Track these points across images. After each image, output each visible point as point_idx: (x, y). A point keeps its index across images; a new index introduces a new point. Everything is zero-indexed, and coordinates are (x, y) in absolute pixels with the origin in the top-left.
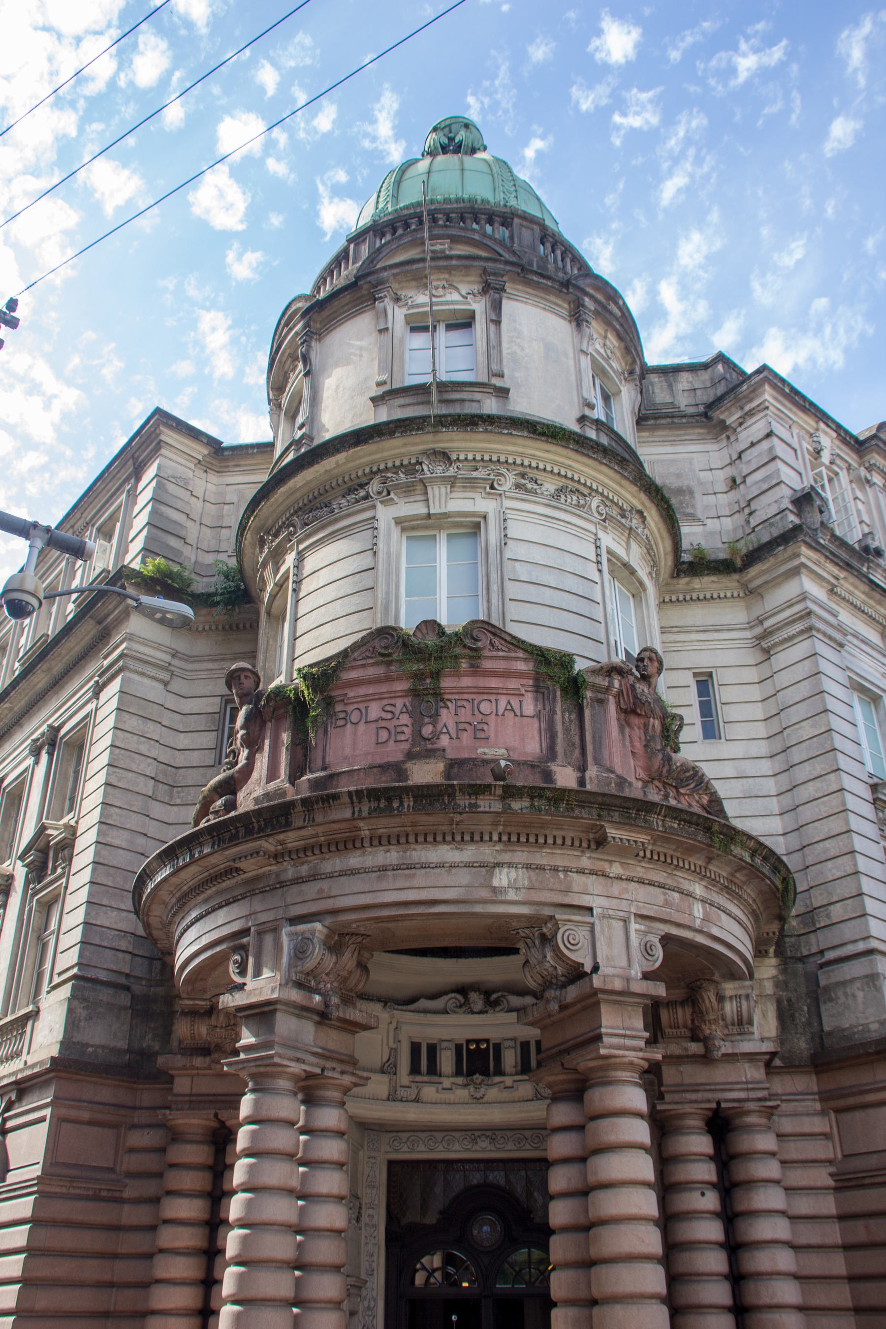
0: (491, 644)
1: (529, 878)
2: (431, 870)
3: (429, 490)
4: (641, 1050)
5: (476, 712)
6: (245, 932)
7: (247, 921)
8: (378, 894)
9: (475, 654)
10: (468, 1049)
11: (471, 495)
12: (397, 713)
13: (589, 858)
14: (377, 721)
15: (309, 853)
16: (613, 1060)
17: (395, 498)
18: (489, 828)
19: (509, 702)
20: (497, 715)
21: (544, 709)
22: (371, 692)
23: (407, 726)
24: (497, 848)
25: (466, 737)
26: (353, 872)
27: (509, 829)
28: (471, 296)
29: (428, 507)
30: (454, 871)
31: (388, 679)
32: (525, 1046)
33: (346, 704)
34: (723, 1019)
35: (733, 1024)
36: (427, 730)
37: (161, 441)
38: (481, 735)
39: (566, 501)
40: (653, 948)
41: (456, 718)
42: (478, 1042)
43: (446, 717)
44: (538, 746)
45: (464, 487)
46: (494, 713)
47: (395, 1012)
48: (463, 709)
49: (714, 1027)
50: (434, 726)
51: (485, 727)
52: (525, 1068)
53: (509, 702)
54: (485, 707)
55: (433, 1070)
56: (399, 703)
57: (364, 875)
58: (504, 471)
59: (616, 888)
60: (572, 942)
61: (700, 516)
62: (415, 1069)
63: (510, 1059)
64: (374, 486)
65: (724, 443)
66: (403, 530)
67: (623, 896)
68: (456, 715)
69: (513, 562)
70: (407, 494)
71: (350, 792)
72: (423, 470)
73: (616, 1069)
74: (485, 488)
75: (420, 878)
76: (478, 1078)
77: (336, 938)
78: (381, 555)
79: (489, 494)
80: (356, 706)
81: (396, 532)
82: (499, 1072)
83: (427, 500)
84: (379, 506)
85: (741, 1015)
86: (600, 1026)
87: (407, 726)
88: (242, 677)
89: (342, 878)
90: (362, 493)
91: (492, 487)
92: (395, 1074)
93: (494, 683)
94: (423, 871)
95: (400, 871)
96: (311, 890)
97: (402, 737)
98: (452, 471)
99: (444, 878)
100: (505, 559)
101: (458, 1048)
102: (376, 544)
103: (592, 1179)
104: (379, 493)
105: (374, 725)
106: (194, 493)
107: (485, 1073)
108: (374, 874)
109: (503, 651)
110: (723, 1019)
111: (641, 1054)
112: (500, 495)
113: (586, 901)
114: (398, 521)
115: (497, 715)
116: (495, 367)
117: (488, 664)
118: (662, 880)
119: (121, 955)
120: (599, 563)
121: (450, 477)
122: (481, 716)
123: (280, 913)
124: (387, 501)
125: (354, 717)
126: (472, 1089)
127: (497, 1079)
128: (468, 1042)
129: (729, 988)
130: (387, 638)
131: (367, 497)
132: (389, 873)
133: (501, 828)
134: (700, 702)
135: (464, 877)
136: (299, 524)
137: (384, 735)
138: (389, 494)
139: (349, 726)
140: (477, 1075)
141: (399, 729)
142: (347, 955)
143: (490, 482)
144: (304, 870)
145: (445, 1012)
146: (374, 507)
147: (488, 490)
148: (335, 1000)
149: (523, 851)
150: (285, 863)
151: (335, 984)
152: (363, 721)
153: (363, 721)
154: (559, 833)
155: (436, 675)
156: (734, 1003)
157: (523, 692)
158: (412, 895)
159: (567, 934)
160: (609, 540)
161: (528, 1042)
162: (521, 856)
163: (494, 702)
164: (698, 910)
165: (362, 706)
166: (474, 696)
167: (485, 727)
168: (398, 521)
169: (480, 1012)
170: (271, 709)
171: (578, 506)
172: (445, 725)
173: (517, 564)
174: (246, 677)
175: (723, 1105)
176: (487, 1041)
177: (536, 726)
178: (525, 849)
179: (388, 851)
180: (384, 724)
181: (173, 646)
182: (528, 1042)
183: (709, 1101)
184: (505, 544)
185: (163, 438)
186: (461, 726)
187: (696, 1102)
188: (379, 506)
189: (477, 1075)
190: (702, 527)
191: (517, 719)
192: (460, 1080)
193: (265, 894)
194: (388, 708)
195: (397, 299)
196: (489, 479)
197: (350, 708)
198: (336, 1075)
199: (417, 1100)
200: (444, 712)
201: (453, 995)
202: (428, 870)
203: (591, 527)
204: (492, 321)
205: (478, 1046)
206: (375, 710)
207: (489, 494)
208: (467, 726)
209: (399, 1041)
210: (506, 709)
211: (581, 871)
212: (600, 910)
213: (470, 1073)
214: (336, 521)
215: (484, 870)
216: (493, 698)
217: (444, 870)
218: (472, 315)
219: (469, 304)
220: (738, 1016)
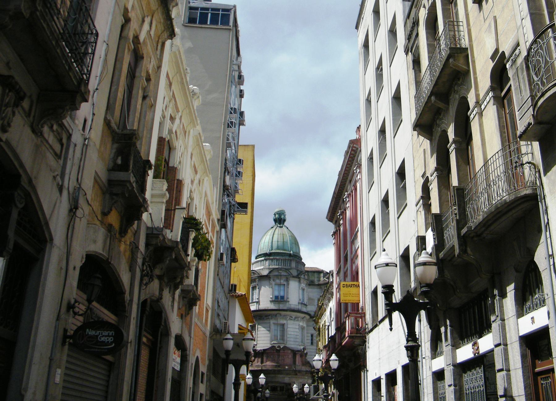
9: (284, 350)
25: (283, 361)
32: (281, 387)
43: (280, 358)
52: (281, 390)
54: (285, 357)
63: (279, 389)
64: (270, 317)
81: (273, 325)
114: (274, 323)
117: (285, 352)
131: (269, 318)
160: (301, 324)
171: (297, 320)
195: (274, 280)
203: (298, 323)
206: (272, 357)
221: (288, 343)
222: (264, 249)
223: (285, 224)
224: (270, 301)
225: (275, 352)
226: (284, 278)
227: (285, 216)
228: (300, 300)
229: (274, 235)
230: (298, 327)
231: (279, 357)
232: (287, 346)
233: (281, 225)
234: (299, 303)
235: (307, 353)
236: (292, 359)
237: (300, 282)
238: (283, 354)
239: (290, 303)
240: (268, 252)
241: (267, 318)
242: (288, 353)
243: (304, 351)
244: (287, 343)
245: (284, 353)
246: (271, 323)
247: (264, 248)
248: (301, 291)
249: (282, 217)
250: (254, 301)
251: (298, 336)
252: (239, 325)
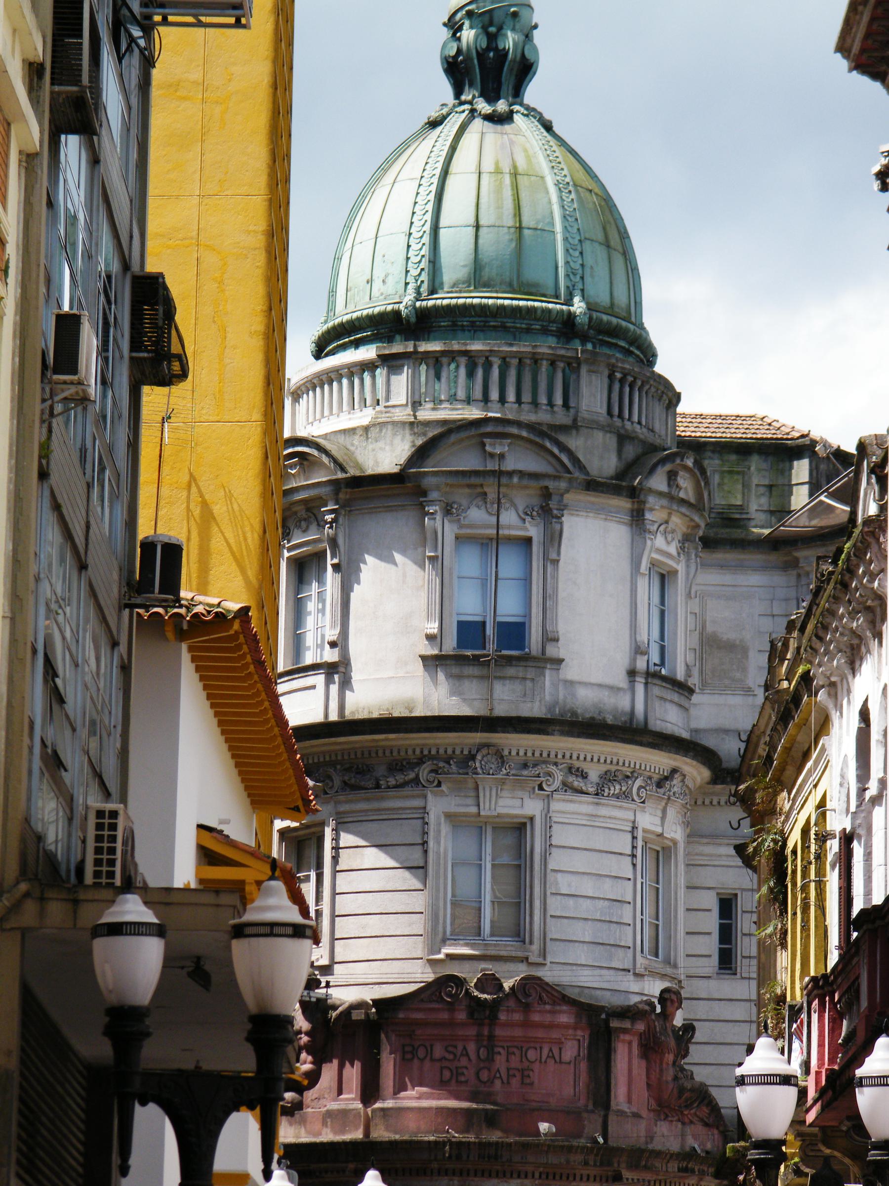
0: (541, 998)
5: (524, 1059)
9: (527, 1008)
14: (440, 1060)
19: (551, 1050)
20: (540, 1062)
25: (515, 1082)
28: (528, 519)
29: (479, 805)
36: (484, 1076)
38: (527, 1081)
43: (500, 1062)
44: (572, 1090)
50: (489, 1070)
51: (531, 1073)
53: (551, 1050)
54: (532, 1055)
58: (552, 768)
61: (751, 685)
64: (424, 772)
65: (793, 580)
74: (534, 788)
78: (431, 855)
79: (538, 794)
81: (445, 829)
91: (541, 788)
93: (540, 1034)
97: (463, 1079)
100: (548, 871)
102: (425, 843)
115: (540, 1062)
117: (536, 1018)
122: (528, 1064)
125: (421, 1053)
131: (416, 781)
133: (541, 1169)
134: (720, 949)
136: (337, 782)
137: (447, 1074)
138: (439, 785)
139: (416, 1061)
146: (425, 797)
152: (428, 1058)
153: (428, 1058)
154: (585, 1172)
172: (498, 1071)
173: (559, 875)
177: (572, 1070)
179: (452, 1180)
180: (446, 1064)
186: (511, 1073)
190: (751, 698)
194: (450, 1049)
195: (448, 511)
200: (497, 1058)
206: (438, 1051)
210: (548, 1057)
216: (538, 1046)
219: (526, 529)
221: (556, 954)
222: (377, 285)
223: (533, 94)
224: (424, 658)
225: (462, 1016)
226: (523, 498)
227: (528, 37)
228: (639, 650)
229: (451, 181)
230: (624, 844)
231: (490, 1059)
232: (548, 975)
233: (502, 106)
234: (632, 673)
235: (689, 1028)
236: (583, 1066)
237: (637, 519)
238: (518, 1032)
239: (570, 672)
240: (406, 302)
241: (400, 778)
242: (552, 1026)
243: (666, 1016)
244: (543, 953)
245: (526, 1024)
246: (432, 818)
247: (378, 275)
248: (647, 590)
249: (510, 40)
250: (309, 659)
251: (628, 909)
252: (200, 827)
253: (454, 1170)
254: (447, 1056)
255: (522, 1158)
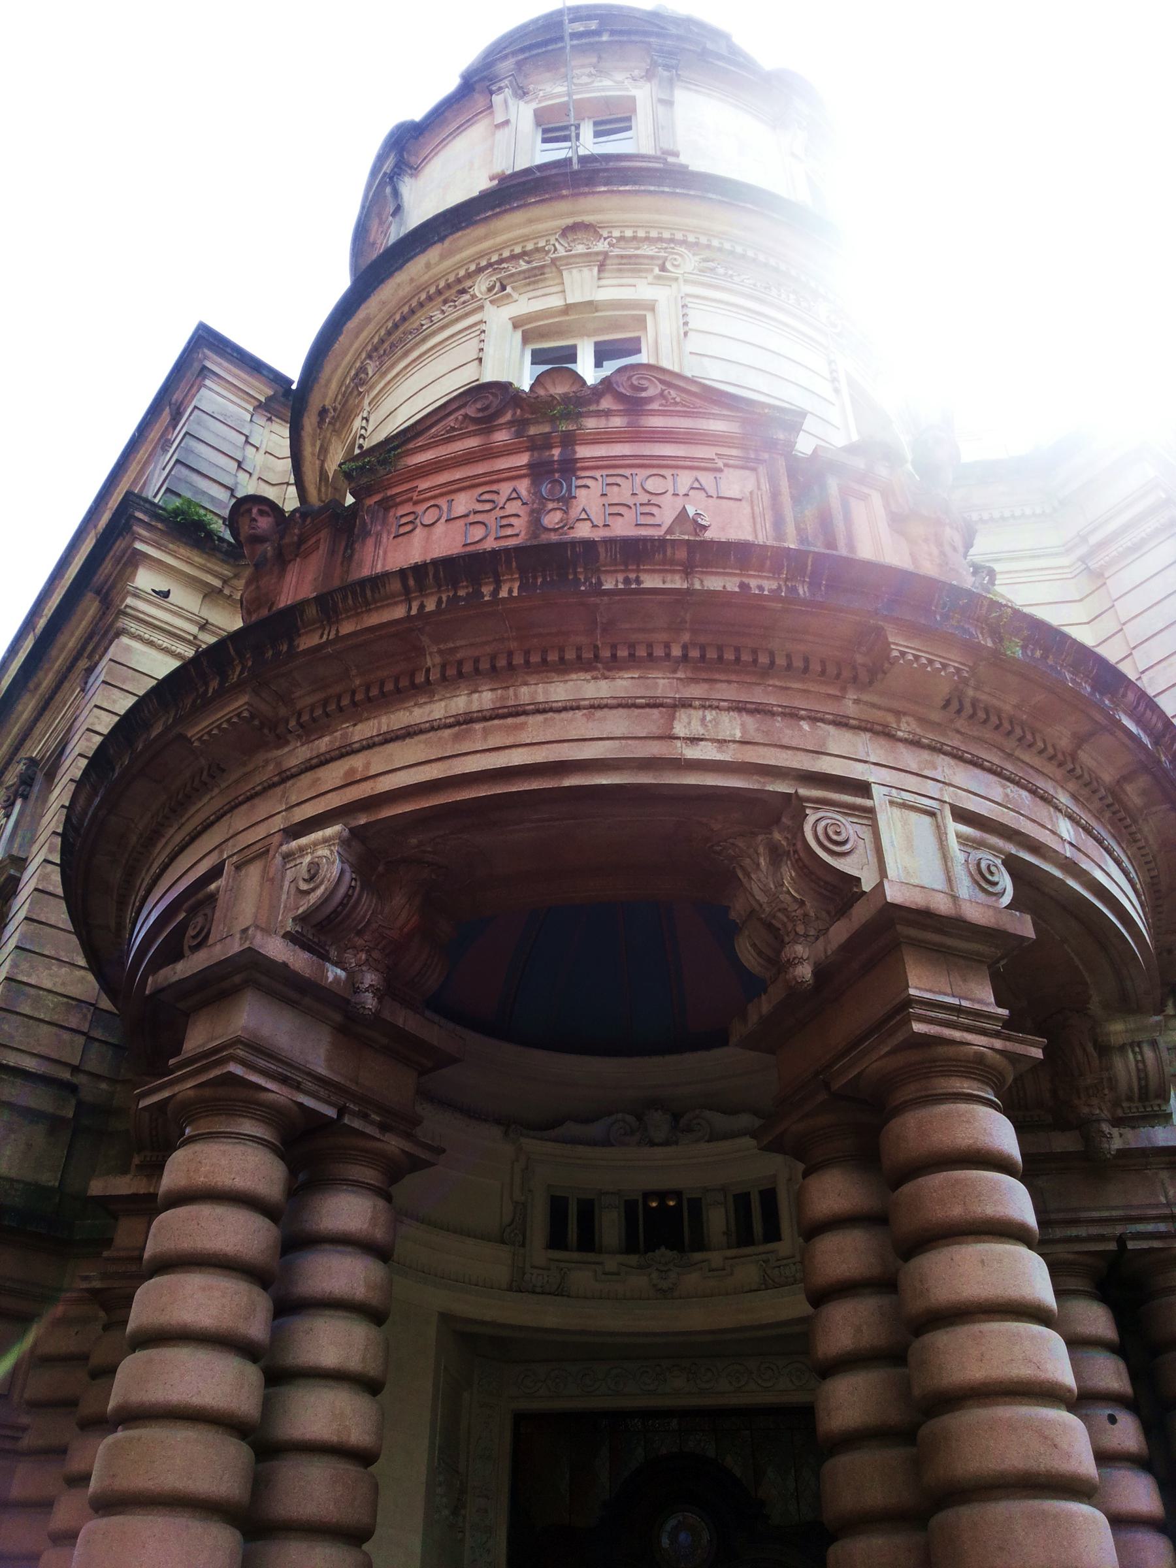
1: (743, 725)
2: (556, 716)
3: (565, 273)
4: (996, 1035)
5: (638, 490)
6: (215, 873)
7: (221, 852)
8: (456, 761)
10: (645, 1205)
11: (631, 281)
12: (501, 500)
13: (857, 701)
14: (466, 516)
15: (332, 707)
16: (942, 1050)
17: (515, 295)
18: (663, 637)
21: (759, 488)
22: (457, 477)
23: (517, 516)
24: (680, 675)
26: (409, 733)
27: (702, 639)
30: (599, 714)
31: (487, 454)
32: (742, 1201)
33: (416, 503)
34: (1113, 1088)
35: (1130, 1099)
37: (204, 368)
39: (780, 295)
40: (993, 869)
41: (605, 500)
42: (662, 1195)
45: (620, 270)
46: (671, 492)
47: (522, 1140)
48: (615, 488)
49: (1095, 1101)
50: (566, 512)
51: (655, 510)
55: (588, 1242)
56: (505, 489)
57: (431, 734)
58: (682, 250)
59: (910, 758)
60: (835, 837)
62: (556, 1241)
63: (717, 1220)
64: (480, 287)
66: (526, 340)
67: (925, 773)
68: (603, 495)
69: (698, 357)
70: (532, 287)
71: (402, 573)
72: (556, 250)
73: (948, 1073)
74: (652, 270)
75: (534, 730)
76: (664, 1254)
77: (381, 868)
79: (658, 277)
80: (432, 503)
82: (700, 1244)
83: (564, 291)
84: (487, 304)
85: (1146, 1077)
86: (908, 986)
87: (517, 516)
88: (255, 511)
89: (391, 747)
90: (466, 297)
91: (663, 268)
92: (523, 1245)
94: (540, 718)
95: (496, 722)
96: (333, 774)
98: (602, 246)
99: (578, 725)
101: (630, 1208)
102: (481, 350)
103: (916, 1306)
104: (490, 290)
105: (461, 523)
106: (251, 441)
107: (677, 1245)
108: (447, 732)
109: (685, 406)
110: (1111, 1089)
111: (998, 1044)
112: (676, 279)
113: (857, 772)
114: (516, 323)
116: (666, 146)
118: (996, 761)
119: (66, 1036)
120: (834, 380)
121: (597, 254)
123: (278, 823)
124: (502, 298)
126: (655, 1275)
127: (698, 1256)
128: (647, 1195)
129: (1117, 1029)
130: (487, 398)
132: (478, 726)
133: (686, 637)
135: (617, 723)
138: (503, 288)
139: (418, 530)
140: (663, 1249)
141: (504, 522)
142: (399, 900)
143: (660, 262)
144: (324, 744)
145: (607, 1143)
147: (657, 270)
148: (370, 978)
149: (729, 682)
150: (289, 737)
151: (376, 954)
152: (443, 520)
155: (569, 441)
156: (1131, 1056)
157: (720, 464)
158: (517, 758)
159: (823, 823)
161: (748, 1194)
162: (726, 692)
163: (670, 478)
164: (1066, 828)
165: (443, 502)
166: (634, 471)
167: (655, 510)
168: (516, 323)
169: (666, 1143)
170: (296, 538)
172: (584, 510)
173: (705, 360)
174: (261, 513)
175: (1131, 1245)
176: (678, 1194)
178: (733, 677)
180: (479, 518)
181: (202, 614)
182: (748, 1194)
183: (1102, 1238)
184: (686, 334)
185: (208, 364)
187: (1078, 1239)
188: (487, 304)
189: (663, 1249)
191: (710, 500)
192: (633, 1259)
193: (256, 801)
194: (486, 497)
195: (522, 93)
196: (658, 258)
197: (420, 509)
198: (369, 1130)
199: (560, 1292)
200: (581, 494)
201: (620, 1116)
202: (550, 715)
204: (661, 101)
205: (662, 1203)
207: (658, 277)
208: (621, 510)
209: (530, 1191)
211: (841, 723)
212: (885, 790)
213: (651, 1247)
214: (424, 340)
215: (655, 711)
217: (579, 714)
218: (630, 104)
220: (1139, 1079)
245: (636, 435)
253: (477, 661)
254: (479, 507)
255: (627, 581)
